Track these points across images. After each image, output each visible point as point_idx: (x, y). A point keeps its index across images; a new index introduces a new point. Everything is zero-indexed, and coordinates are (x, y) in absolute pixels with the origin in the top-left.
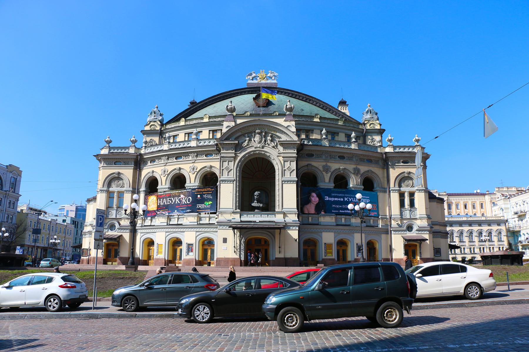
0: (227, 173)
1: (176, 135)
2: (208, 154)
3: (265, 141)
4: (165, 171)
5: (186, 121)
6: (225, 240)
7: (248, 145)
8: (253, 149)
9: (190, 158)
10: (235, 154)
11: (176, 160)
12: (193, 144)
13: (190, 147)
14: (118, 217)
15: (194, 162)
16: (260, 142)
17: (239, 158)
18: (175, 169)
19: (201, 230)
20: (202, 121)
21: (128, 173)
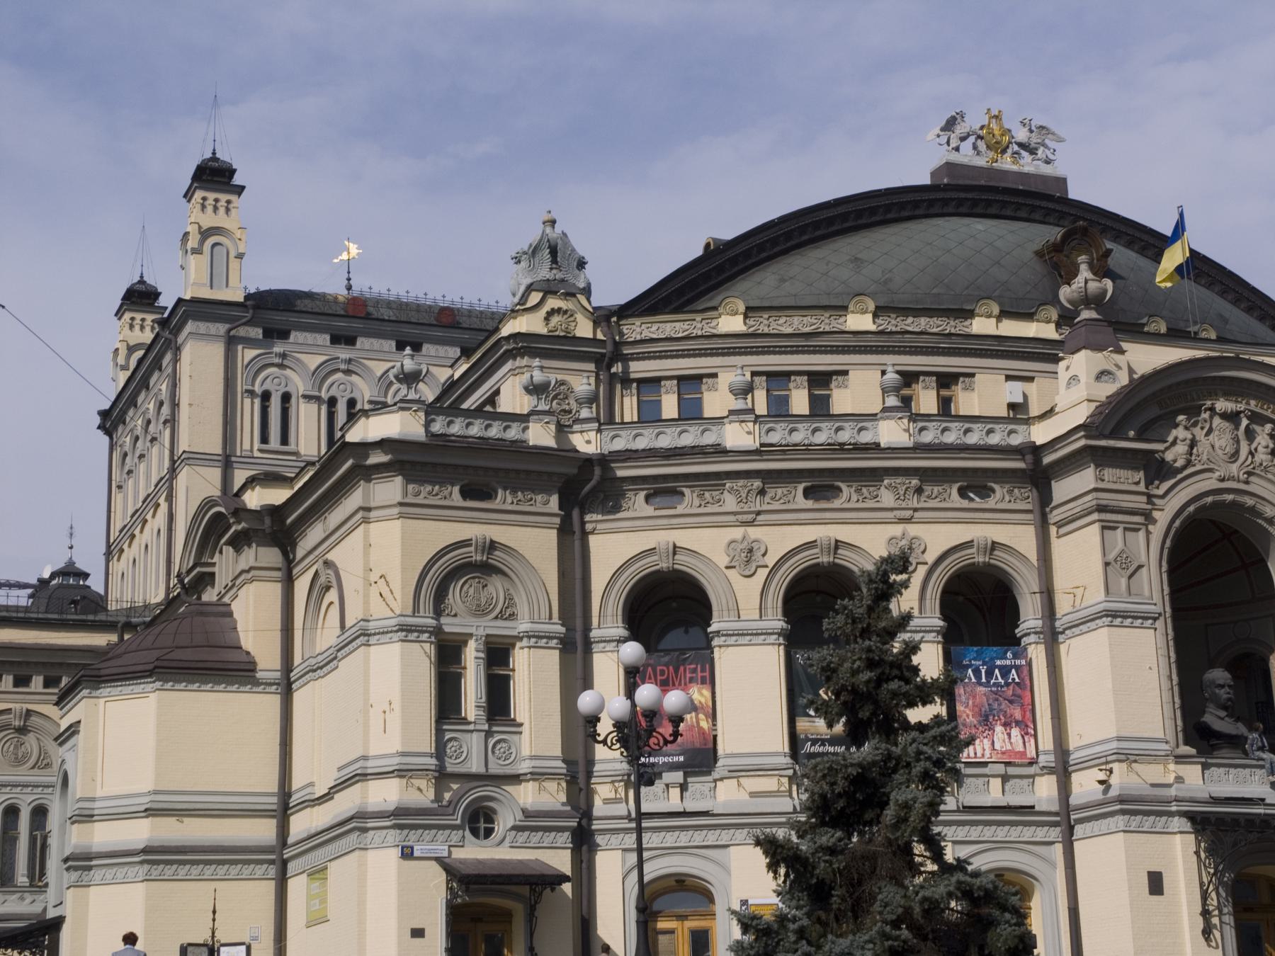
0: (1124, 581)
1: (699, 378)
2: (975, 484)
3: (1251, 453)
4: (751, 551)
5: (750, 311)
6: (1156, 883)
7: (1189, 463)
8: (1210, 483)
9: (887, 498)
10: (1150, 496)
11: (810, 504)
12: (892, 433)
13: (876, 447)
14: (495, 769)
15: (908, 520)
16: (1235, 456)
17: (1163, 518)
18: (811, 545)
19: (975, 833)
20: (836, 325)
21: (533, 543)
